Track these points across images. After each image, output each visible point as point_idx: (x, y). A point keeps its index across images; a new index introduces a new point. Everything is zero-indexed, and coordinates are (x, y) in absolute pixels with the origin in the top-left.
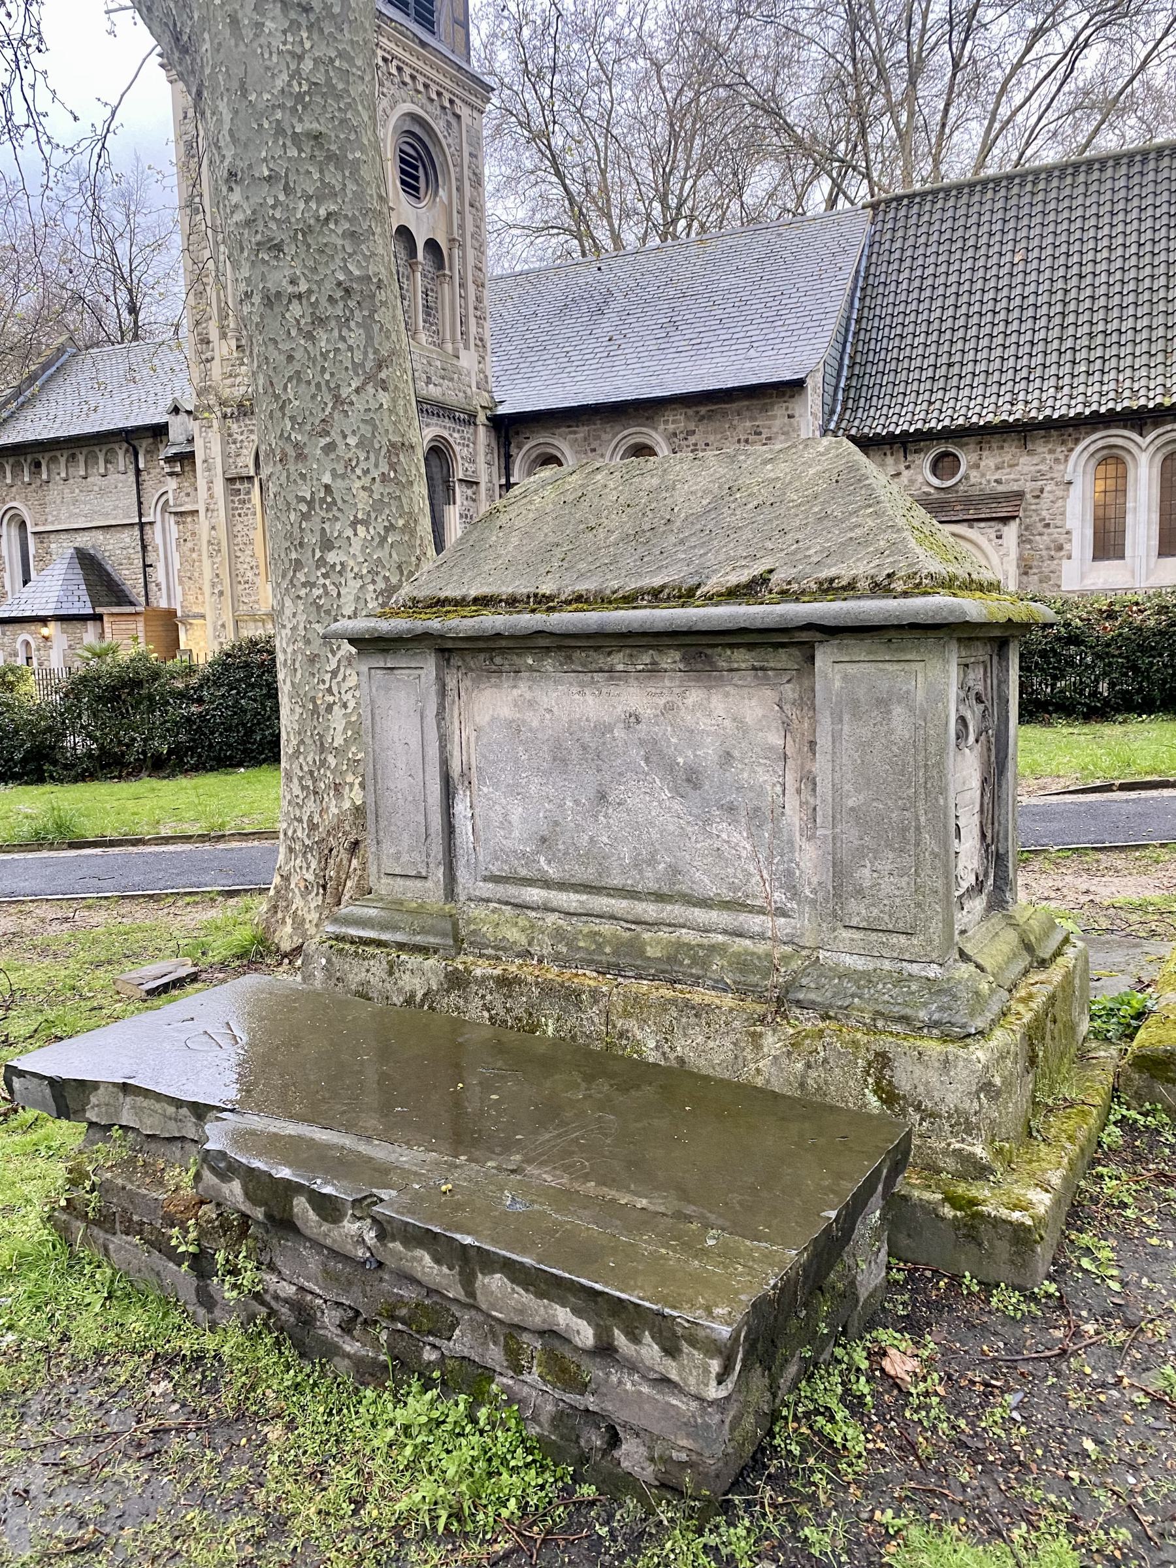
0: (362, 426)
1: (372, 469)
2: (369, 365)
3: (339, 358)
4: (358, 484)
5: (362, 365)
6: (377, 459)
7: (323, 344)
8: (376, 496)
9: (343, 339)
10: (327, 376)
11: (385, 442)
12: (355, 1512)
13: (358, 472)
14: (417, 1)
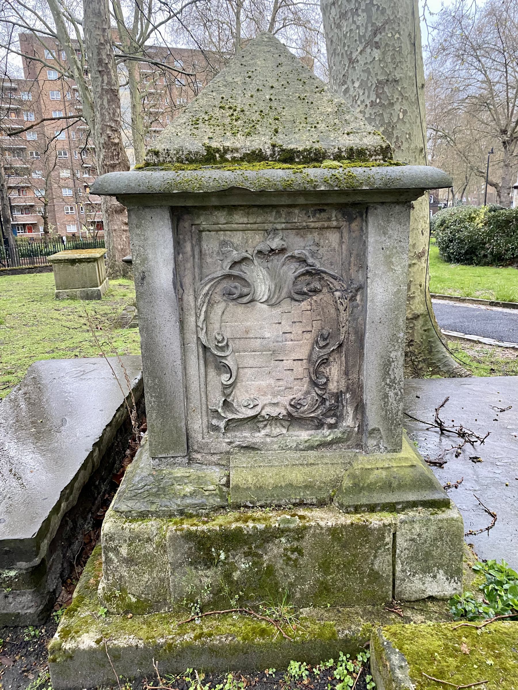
0: (362, 74)
1: (366, 100)
2: (369, 33)
3: (352, 35)
4: (358, 110)
5: (364, 36)
6: (369, 93)
7: (345, 29)
8: (367, 116)
9: (354, 22)
10: (346, 48)
11: (375, 81)
12: (77, 91)
13: (359, 102)
14: (252, 1)
